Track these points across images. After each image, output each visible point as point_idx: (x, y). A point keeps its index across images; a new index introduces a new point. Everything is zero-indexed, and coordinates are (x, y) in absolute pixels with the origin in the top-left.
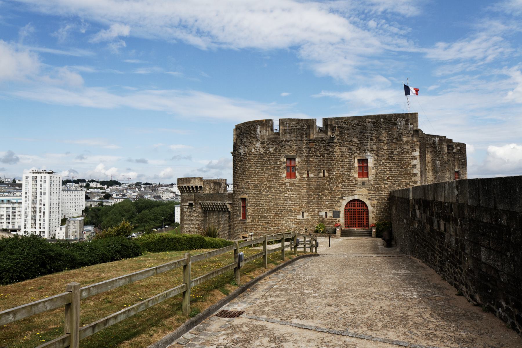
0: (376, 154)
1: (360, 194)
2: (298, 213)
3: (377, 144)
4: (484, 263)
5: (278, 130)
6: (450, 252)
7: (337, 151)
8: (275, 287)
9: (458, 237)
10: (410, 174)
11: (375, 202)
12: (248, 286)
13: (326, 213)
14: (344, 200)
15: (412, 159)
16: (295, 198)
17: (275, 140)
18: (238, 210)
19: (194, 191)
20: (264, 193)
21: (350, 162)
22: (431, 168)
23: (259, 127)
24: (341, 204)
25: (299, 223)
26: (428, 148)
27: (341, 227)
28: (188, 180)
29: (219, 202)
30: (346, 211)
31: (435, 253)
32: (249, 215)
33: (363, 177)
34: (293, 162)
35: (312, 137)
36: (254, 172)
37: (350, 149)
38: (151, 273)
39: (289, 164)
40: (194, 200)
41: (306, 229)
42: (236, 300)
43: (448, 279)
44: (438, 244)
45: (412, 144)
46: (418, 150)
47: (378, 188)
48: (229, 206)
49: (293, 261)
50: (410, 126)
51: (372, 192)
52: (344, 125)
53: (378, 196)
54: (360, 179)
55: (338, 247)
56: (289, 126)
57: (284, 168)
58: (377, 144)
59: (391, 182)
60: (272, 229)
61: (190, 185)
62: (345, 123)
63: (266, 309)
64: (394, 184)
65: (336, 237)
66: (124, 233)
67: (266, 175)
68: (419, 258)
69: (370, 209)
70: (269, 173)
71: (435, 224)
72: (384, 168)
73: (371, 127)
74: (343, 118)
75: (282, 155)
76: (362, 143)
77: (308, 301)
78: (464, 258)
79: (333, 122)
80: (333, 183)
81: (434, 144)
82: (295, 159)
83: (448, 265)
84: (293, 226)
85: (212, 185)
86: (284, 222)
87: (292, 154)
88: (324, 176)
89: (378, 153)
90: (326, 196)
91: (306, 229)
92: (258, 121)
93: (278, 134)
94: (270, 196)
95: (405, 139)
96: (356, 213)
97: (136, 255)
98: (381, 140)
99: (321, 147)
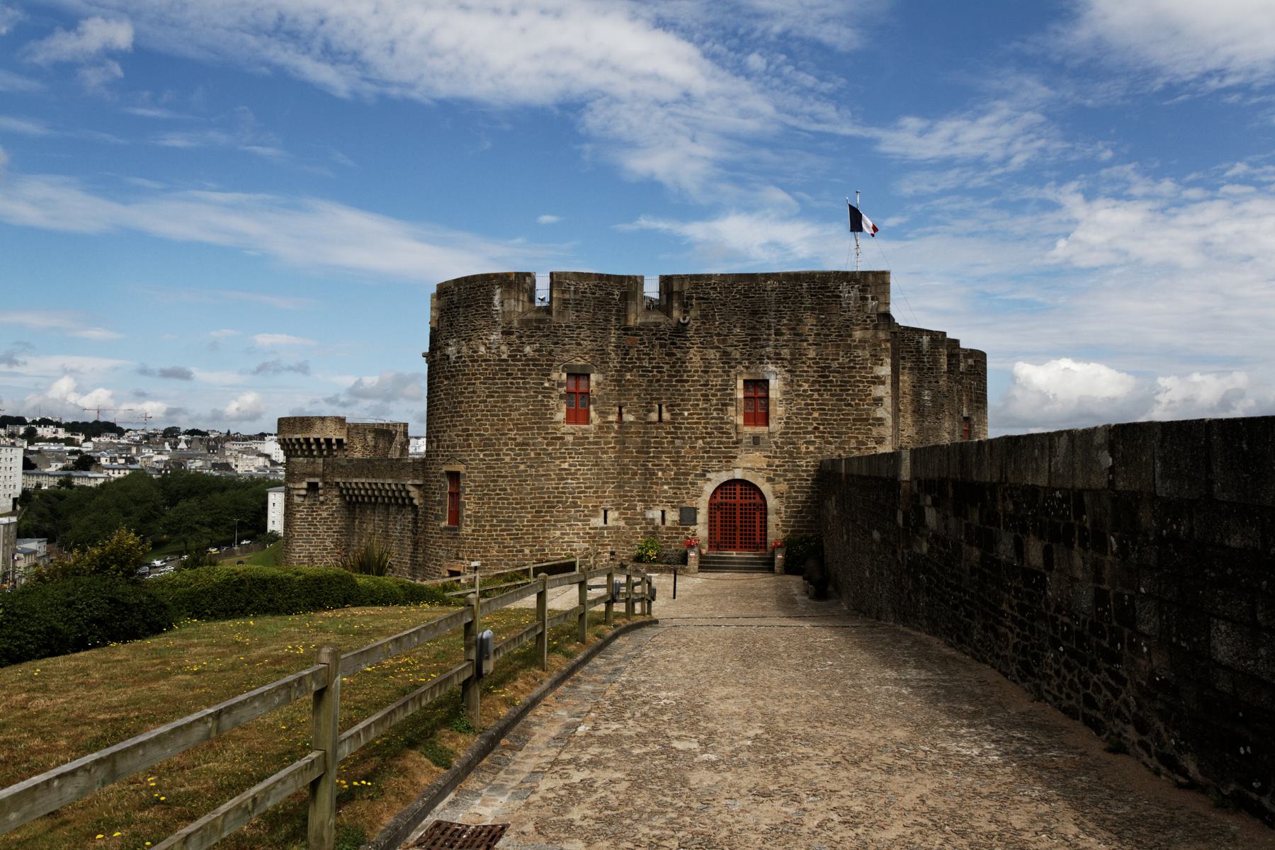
0: (789, 367)
1: (748, 466)
2: (595, 512)
3: (791, 344)
4: (1227, 668)
5: (548, 299)
6: (1063, 624)
7: (694, 358)
8: (582, 729)
9: (1106, 587)
10: (867, 420)
11: (783, 487)
12: (502, 732)
13: (663, 512)
14: (709, 480)
15: (874, 383)
16: (586, 473)
17: (540, 324)
18: (440, 503)
19: (321, 451)
20: (507, 459)
21: (726, 387)
22: (910, 408)
23: (498, 291)
24: (701, 490)
25: (595, 537)
26: (903, 358)
27: (700, 547)
28: (305, 422)
29: (390, 481)
30: (713, 507)
31: (1000, 623)
32: (468, 516)
33: (756, 425)
34: (583, 382)
35: (633, 321)
36: (482, 406)
37: (725, 353)
38: (200, 731)
39: (572, 388)
40: (323, 476)
41: (612, 553)
42: (472, 783)
43: (1056, 698)
44: (1015, 602)
45: (876, 345)
46: (889, 360)
47: (791, 453)
48: (414, 493)
49: (603, 646)
50: (872, 304)
51: (777, 462)
52: (713, 294)
53: (792, 471)
54: (749, 430)
55: (696, 597)
56: (575, 292)
57: (561, 397)
58: (791, 344)
59: (823, 437)
60: (527, 551)
61: (312, 436)
62: (715, 289)
63: (575, 814)
64: (830, 443)
65: (687, 572)
66: (122, 564)
67: (515, 415)
68: (935, 634)
69: (772, 503)
70: (521, 409)
71: (1005, 549)
72: (807, 404)
73: (779, 302)
74: (710, 277)
75: (555, 364)
76: (754, 340)
77: (695, 778)
78: (1135, 648)
79: (686, 286)
80: (683, 438)
81: (919, 350)
82: (588, 376)
83: (1056, 660)
84: (580, 545)
85: (369, 437)
86: (558, 533)
87: (582, 362)
88: (660, 419)
89: (792, 367)
90: (663, 471)
91: (612, 553)
92: (496, 275)
93: (548, 310)
94: (522, 467)
95: (858, 334)
96: (737, 512)
97: (155, 629)
98: (801, 335)
99: (653, 346)
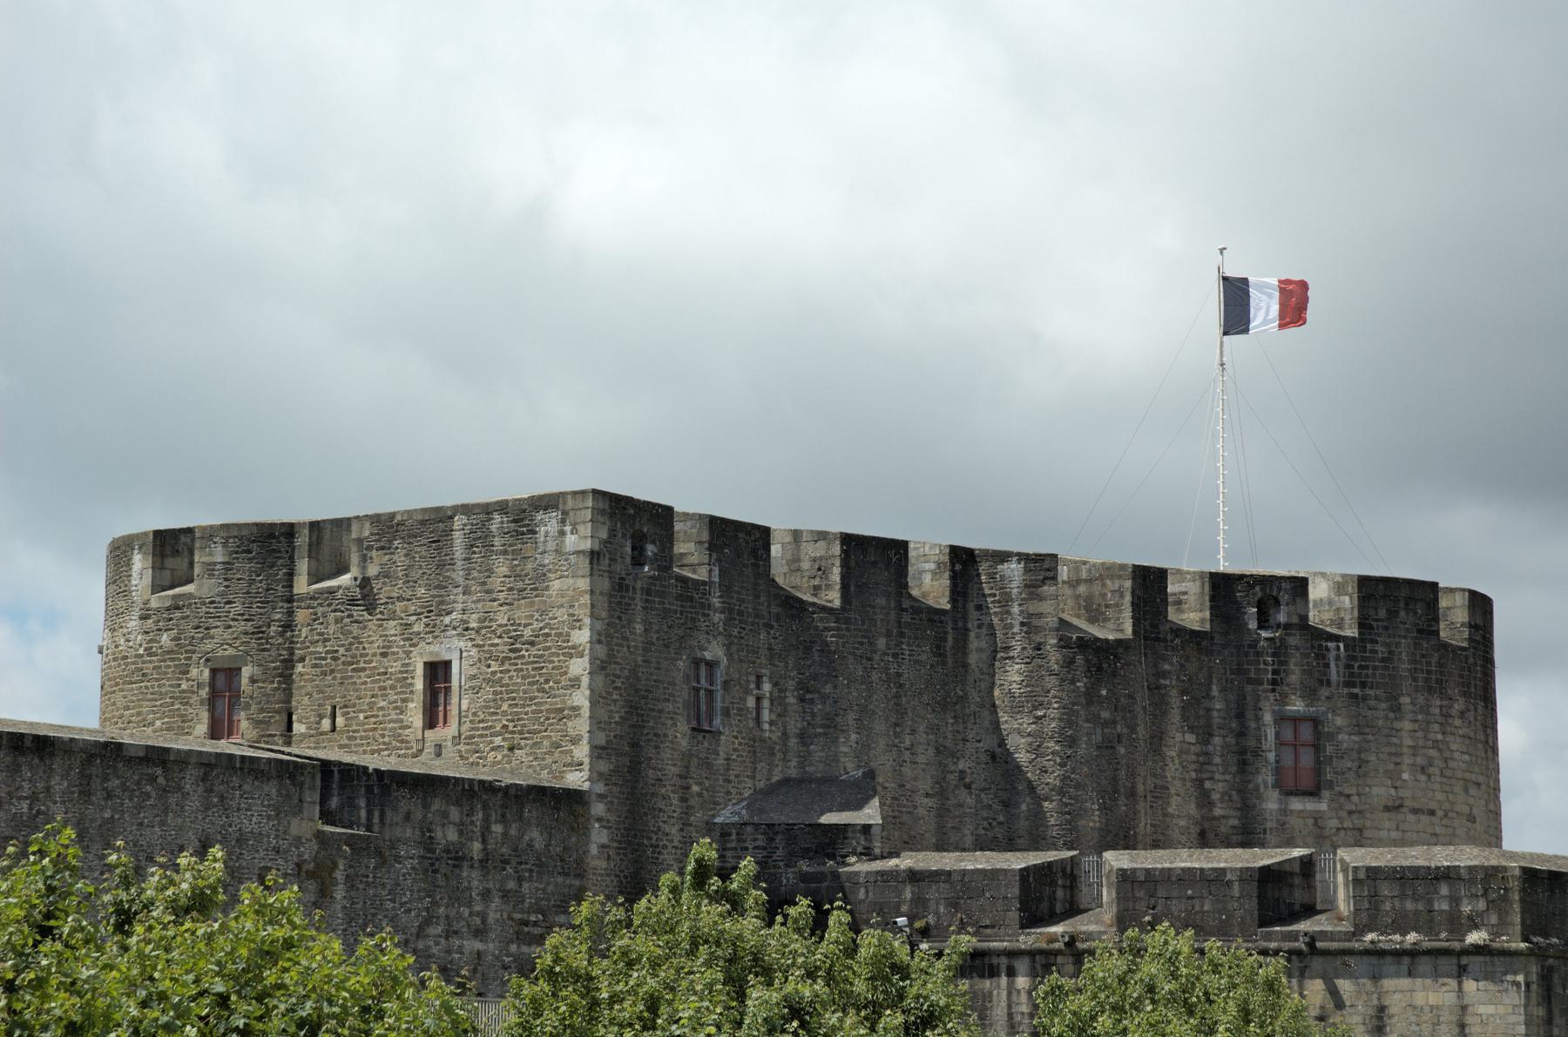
10: (562, 710)
88: (334, 729)
